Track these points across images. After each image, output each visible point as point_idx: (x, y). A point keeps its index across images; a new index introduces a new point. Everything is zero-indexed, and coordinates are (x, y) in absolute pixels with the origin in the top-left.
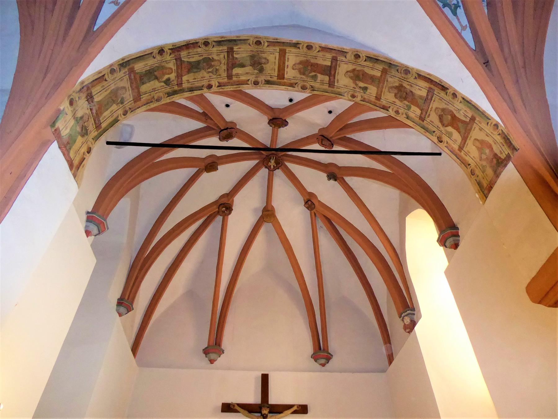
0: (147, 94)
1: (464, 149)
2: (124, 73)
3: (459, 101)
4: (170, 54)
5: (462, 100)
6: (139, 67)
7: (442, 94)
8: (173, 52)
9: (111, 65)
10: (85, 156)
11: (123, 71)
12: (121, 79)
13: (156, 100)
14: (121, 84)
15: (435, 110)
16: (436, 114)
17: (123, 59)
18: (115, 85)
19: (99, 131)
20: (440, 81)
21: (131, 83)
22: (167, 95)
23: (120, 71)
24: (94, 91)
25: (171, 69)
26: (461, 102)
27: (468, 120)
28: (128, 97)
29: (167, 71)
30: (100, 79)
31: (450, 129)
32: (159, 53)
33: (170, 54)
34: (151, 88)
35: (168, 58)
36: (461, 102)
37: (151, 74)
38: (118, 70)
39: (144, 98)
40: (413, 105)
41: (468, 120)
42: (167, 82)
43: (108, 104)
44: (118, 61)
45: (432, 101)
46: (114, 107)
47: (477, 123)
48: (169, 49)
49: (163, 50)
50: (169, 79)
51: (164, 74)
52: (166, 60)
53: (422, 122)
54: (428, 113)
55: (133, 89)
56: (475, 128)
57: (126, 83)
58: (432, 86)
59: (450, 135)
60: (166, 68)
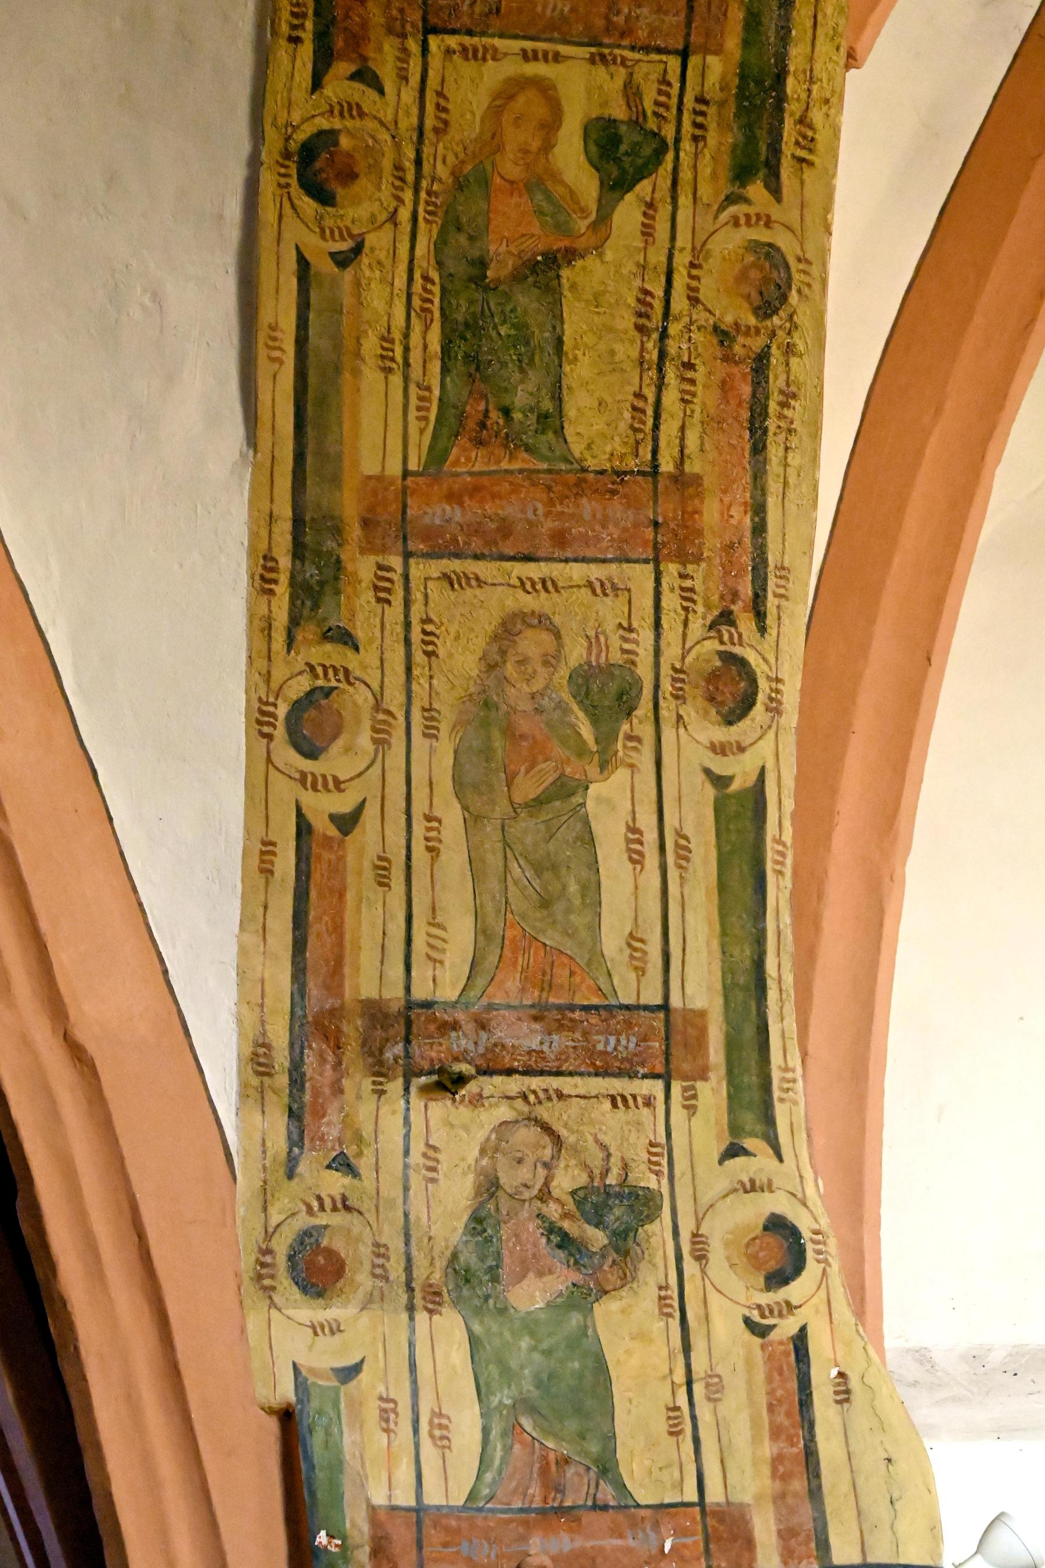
0: (671, 398)
2: (382, 594)
4: (366, 76)
6: (382, 431)
8: (357, 41)
9: (260, 720)
10: (788, 1327)
11: (361, 609)
12: (421, 643)
13: (766, 309)
14: (462, 658)
17: (264, 579)
18: (431, 733)
19: (716, 1053)
21: (499, 543)
22: (756, 190)
23: (346, 639)
24: (372, 976)
25: (507, 93)
28: (609, 611)
29: (514, 138)
30: (305, 875)
32: (324, 197)
33: (366, 76)
34: (627, 351)
35: (398, 102)
37: (490, 325)
38: (332, 653)
39: (694, 435)
42: (623, 154)
43: (545, 867)
44: (261, 627)
46: (612, 801)
48: (317, 84)
49: (308, 153)
50: (605, 141)
51: (539, 182)
52: (408, 122)
55: (563, 545)
57: (468, 609)
60: (492, 142)
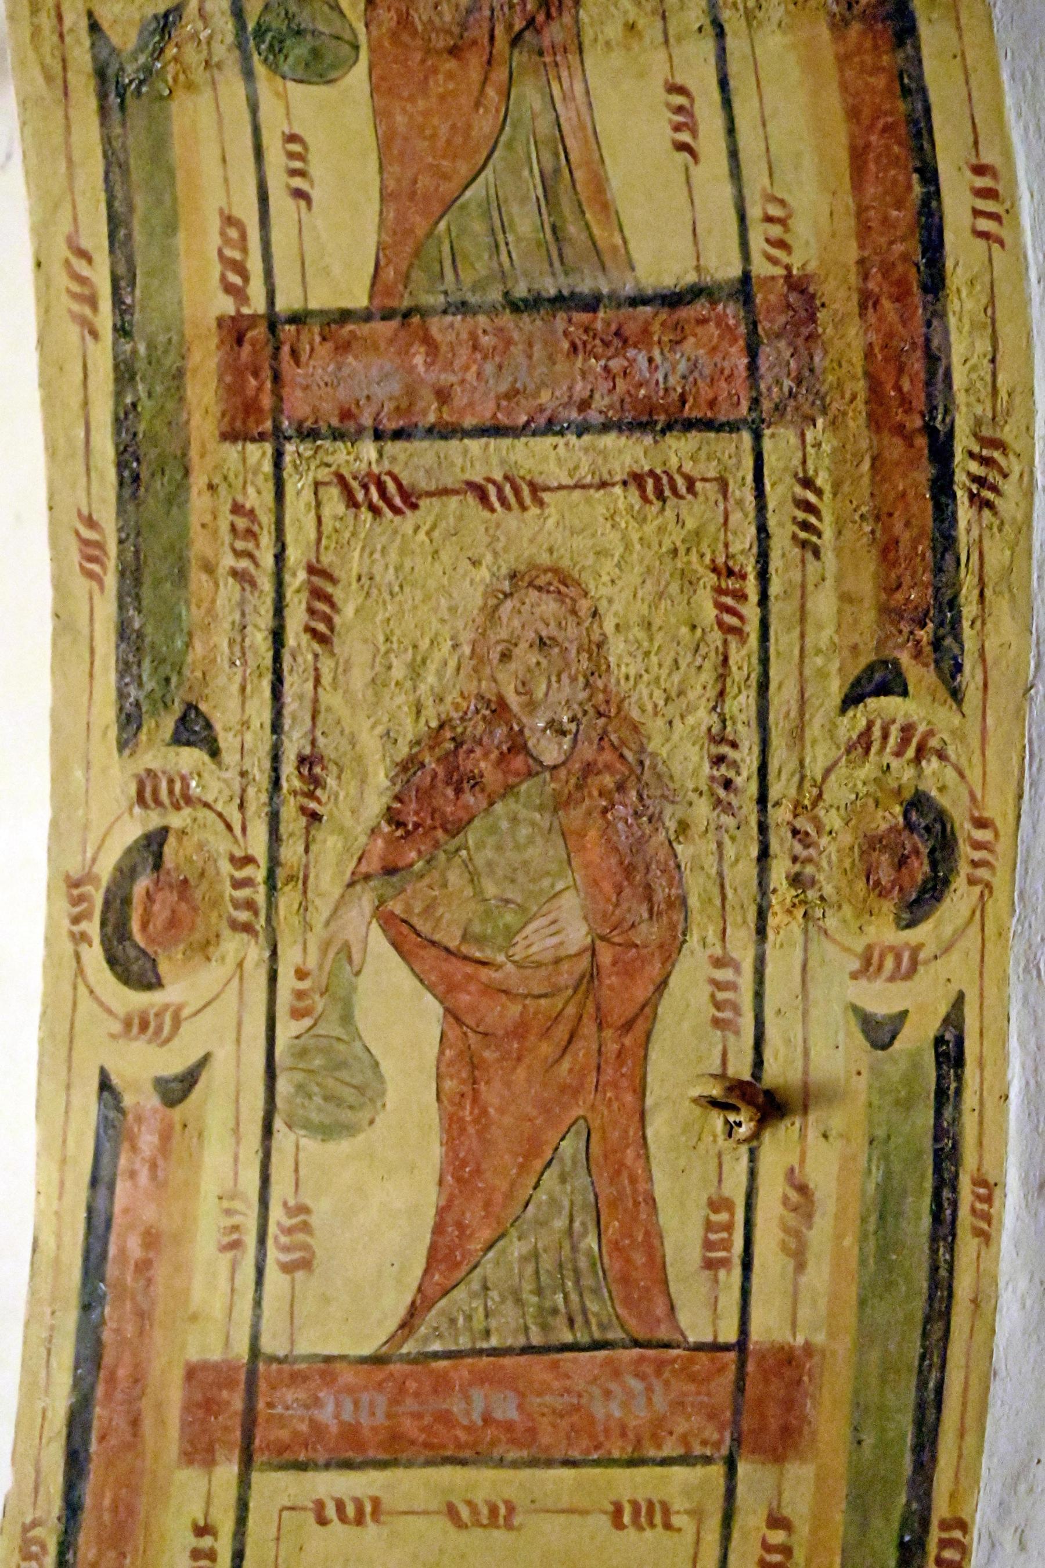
1: (272, 1487)
3: (881, 999)
5: (918, 1037)
7: (828, 611)
15: (520, 580)
16: (488, 652)
20: (991, 446)
26: (881, 1033)
27: (696, 1326)
31: (400, 1021)
36: (881, 1033)
40: (380, 86)
41: (702, 1314)
45: (627, 452)
47: (751, 1519)
53: (204, 398)
54: (415, 461)
56: (652, 1514)
58: (847, 340)
59: (312, 1081)
